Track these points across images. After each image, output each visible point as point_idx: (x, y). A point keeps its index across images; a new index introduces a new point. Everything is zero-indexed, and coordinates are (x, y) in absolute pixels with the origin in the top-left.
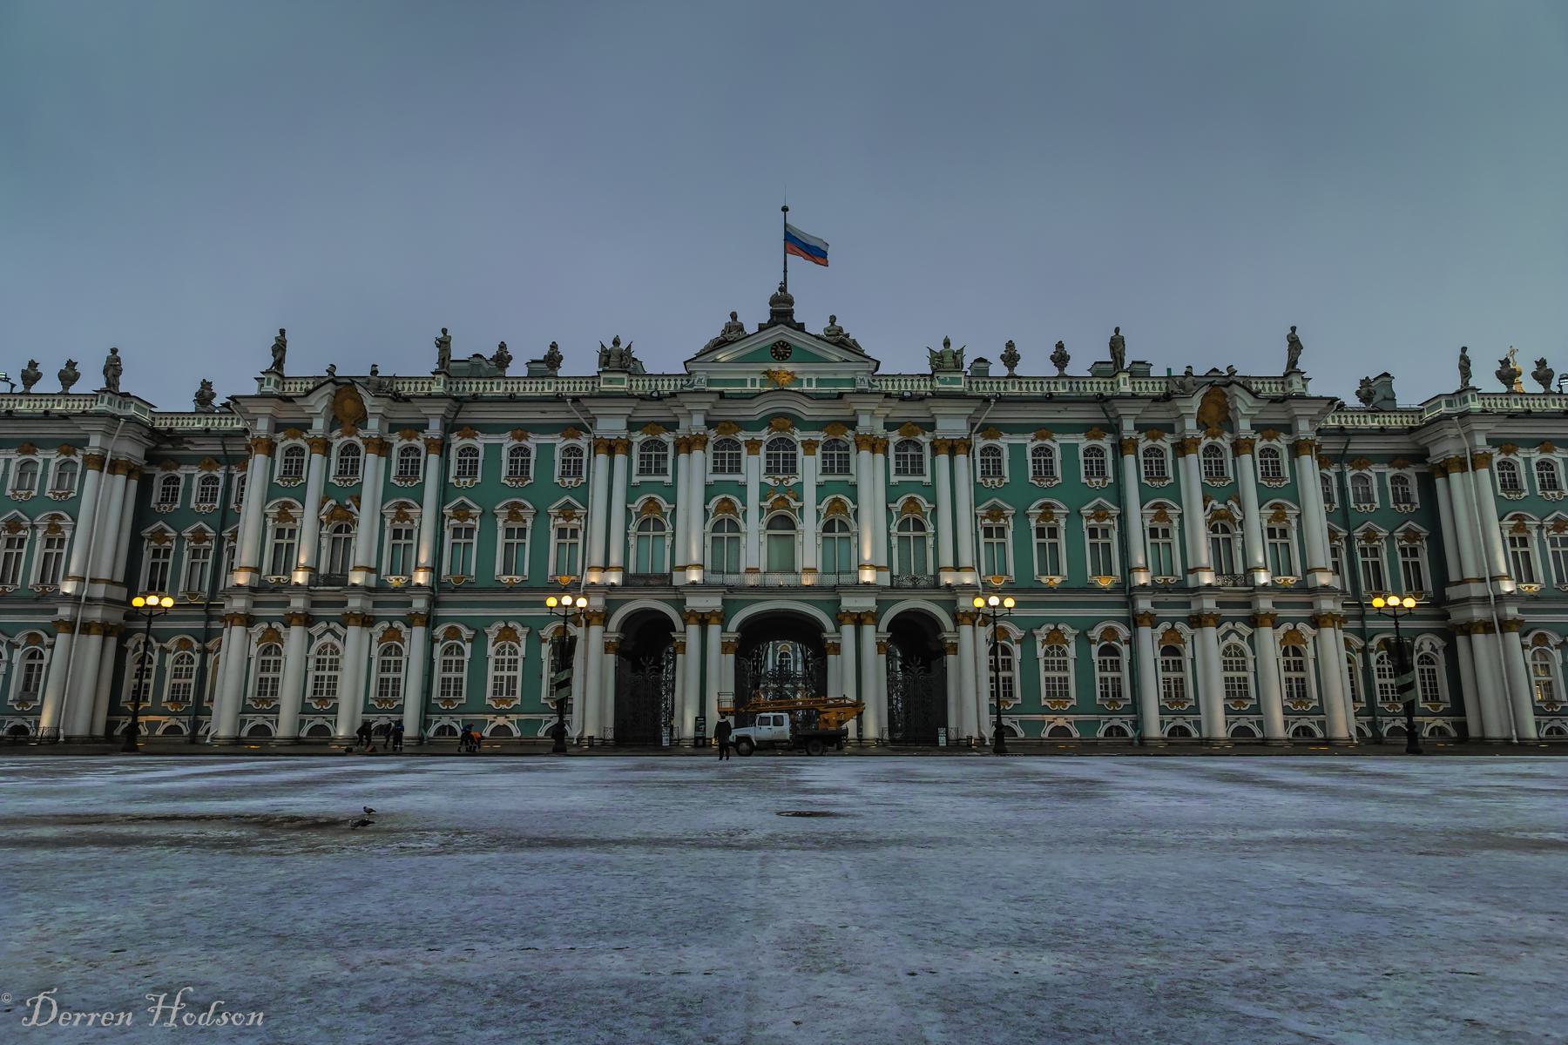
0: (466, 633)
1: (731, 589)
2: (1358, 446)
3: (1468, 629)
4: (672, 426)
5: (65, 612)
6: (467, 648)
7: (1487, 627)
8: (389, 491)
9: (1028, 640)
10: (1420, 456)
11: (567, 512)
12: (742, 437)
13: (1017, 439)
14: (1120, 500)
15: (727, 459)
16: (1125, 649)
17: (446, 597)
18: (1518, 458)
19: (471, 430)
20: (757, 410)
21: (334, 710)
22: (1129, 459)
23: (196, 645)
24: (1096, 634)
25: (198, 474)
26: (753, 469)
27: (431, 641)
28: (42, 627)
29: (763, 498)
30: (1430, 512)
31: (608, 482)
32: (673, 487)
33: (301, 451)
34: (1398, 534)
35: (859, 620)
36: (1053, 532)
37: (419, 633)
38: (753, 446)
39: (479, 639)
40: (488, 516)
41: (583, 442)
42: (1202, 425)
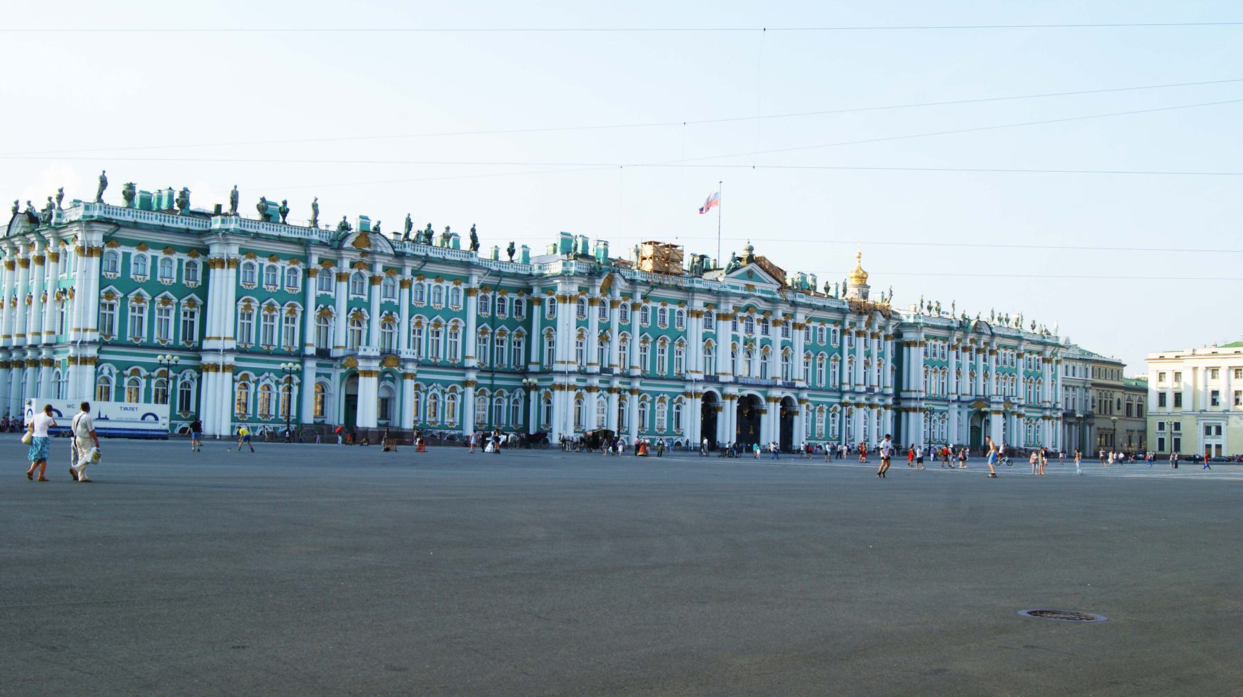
0: (649, 398)
3: (908, 410)
4: (716, 306)
7: (915, 410)
9: (813, 411)
10: (898, 335)
12: (740, 314)
14: (841, 354)
17: (645, 381)
20: (747, 302)
23: (488, 393)
28: (458, 382)
29: (745, 344)
35: (776, 400)
38: (742, 318)
41: (685, 310)
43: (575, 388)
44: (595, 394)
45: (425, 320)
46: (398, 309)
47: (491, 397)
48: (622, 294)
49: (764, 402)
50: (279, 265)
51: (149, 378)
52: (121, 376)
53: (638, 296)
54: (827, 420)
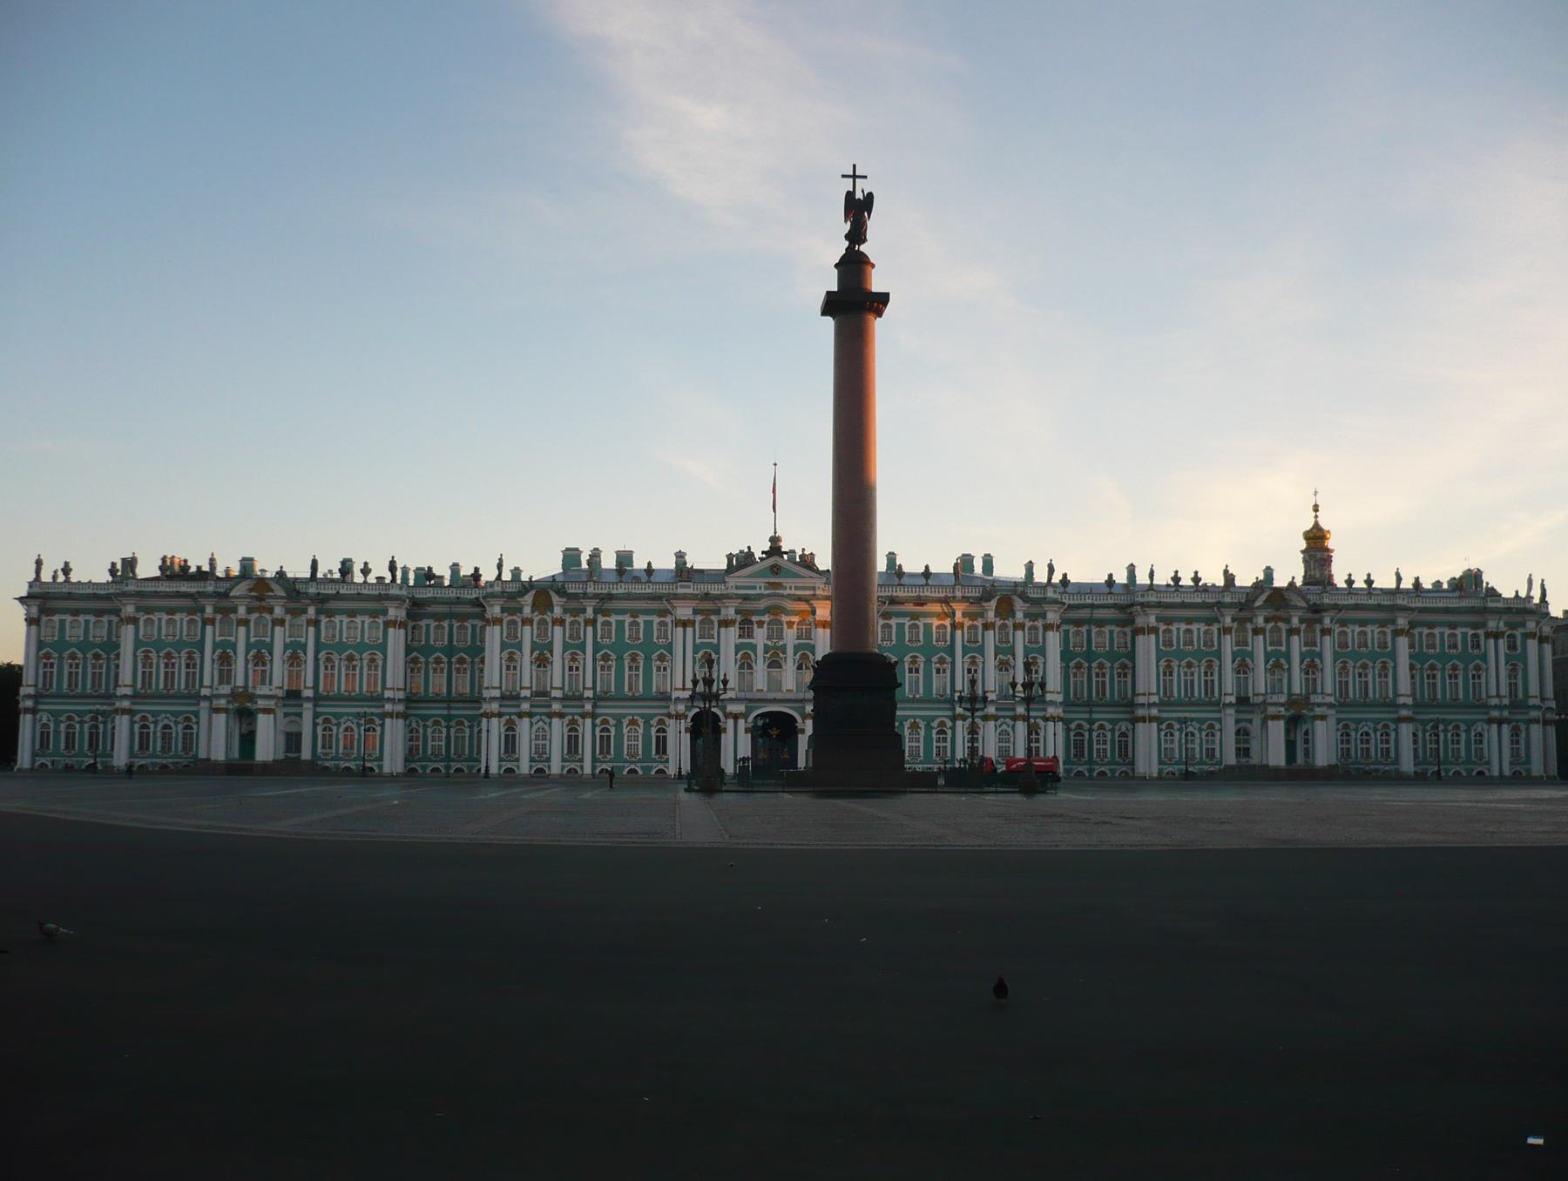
0: (612, 722)
1: (750, 700)
2: (1099, 614)
4: (718, 612)
5: (388, 707)
6: (613, 730)
7: (1143, 720)
8: (566, 646)
11: (662, 658)
12: (754, 619)
13: (901, 620)
14: (952, 655)
15: (746, 628)
16: (949, 732)
18: (1174, 628)
19: (606, 613)
20: (763, 604)
21: (548, 760)
22: (959, 632)
24: (935, 724)
25: (433, 624)
26: (760, 637)
27: (594, 726)
28: (377, 715)
29: (766, 652)
30: (1132, 656)
31: (683, 642)
32: (718, 644)
33: (515, 622)
34: (1116, 665)
36: (917, 671)
37: (588, 721)
38: (760, 624)
39: (619, 725)
40: (620, 659)
41: (668, 619)
42: (998, 613)
43: (500, 715)
44: (526, 720)
45: (335, 657)
46: (304, 647)
47: (448, 728)
48: (565, 611)
49: (799, 719)
50: (177, 617)
51: (82, 723)
52: (57, 723)
53: (590, 611)
54: (928, 738)
